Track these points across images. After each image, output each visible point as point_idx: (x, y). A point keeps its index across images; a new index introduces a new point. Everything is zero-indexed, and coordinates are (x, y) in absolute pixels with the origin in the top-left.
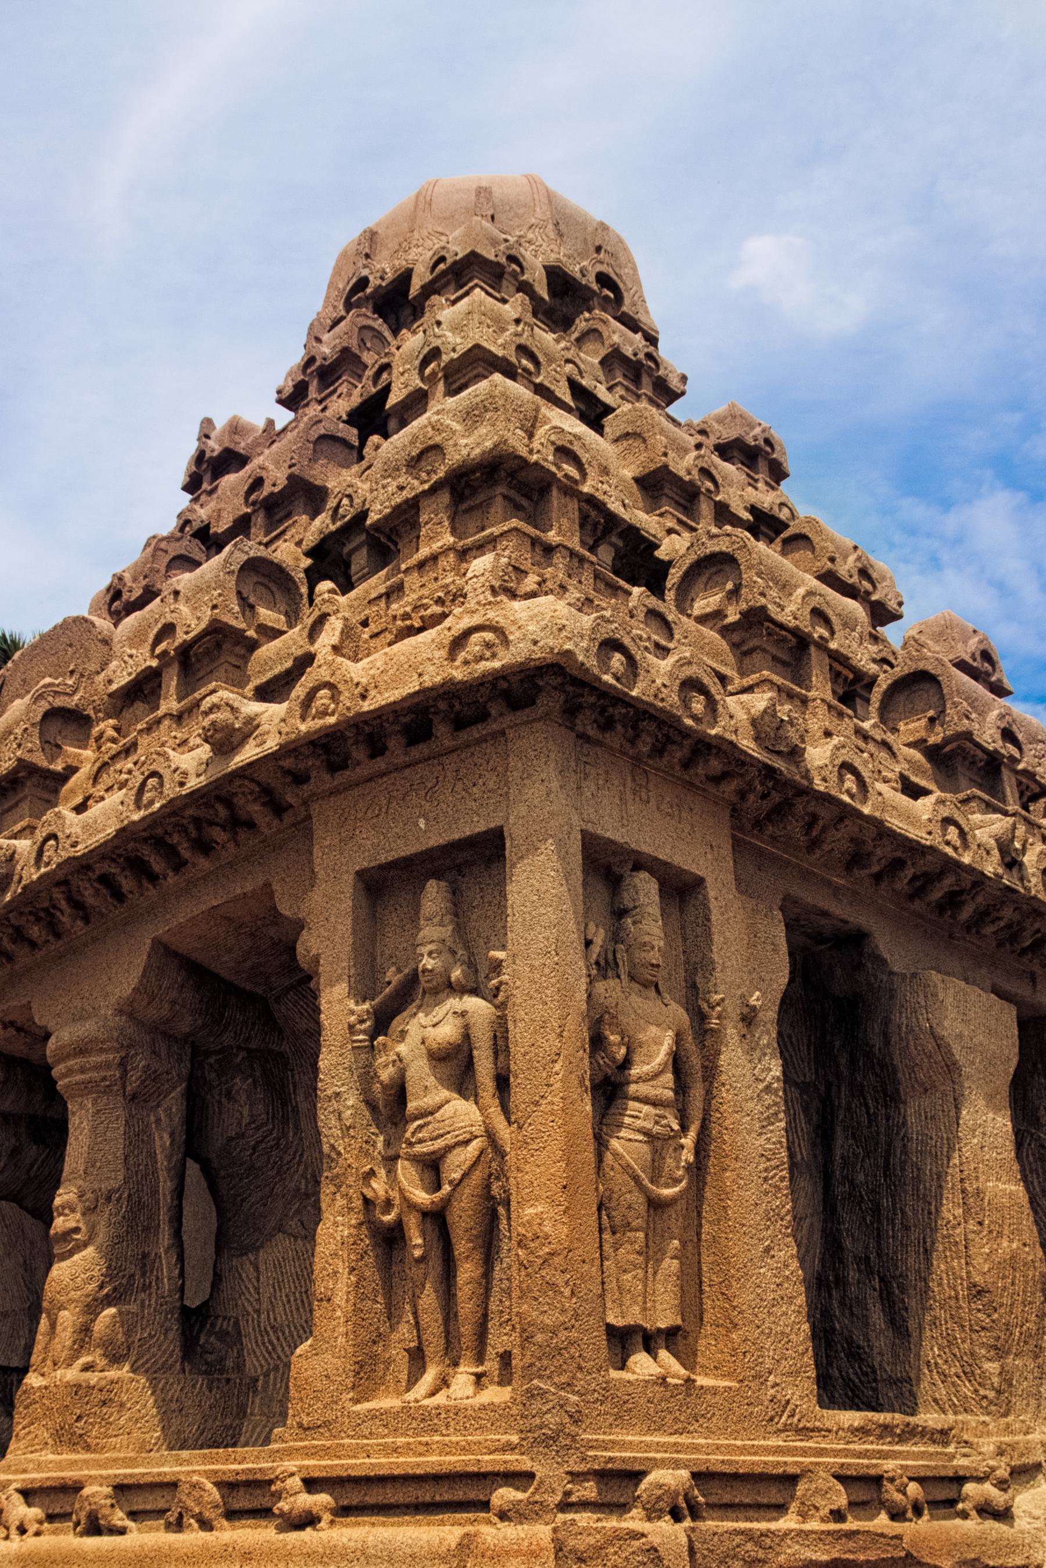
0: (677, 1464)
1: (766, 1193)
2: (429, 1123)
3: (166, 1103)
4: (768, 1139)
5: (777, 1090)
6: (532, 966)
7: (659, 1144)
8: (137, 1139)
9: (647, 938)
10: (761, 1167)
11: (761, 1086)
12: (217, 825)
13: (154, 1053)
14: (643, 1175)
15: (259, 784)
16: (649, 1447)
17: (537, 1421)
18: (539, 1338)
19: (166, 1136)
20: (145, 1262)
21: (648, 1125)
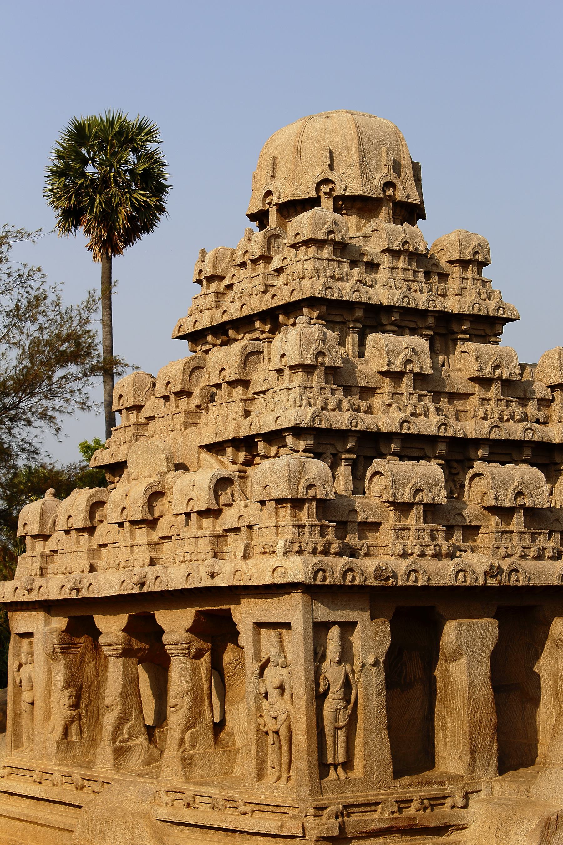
0: (338, 804)
8: (195, 672)
16: (331, 799)
17: (300, 794)
18: (300, 772)
20: (200, 713)
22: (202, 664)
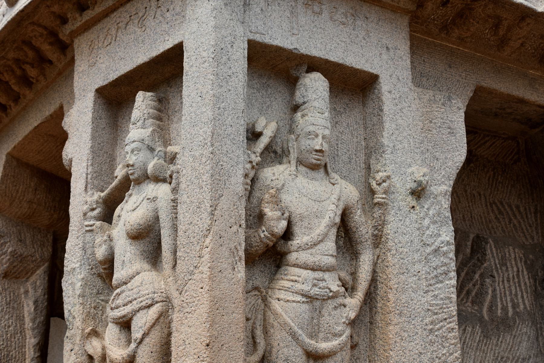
1: (432, 343)
2: (122, 292)
3: (33, 278)
4: (435, 296)
5: (445, 254)
6: (194, 156)
7: (317, 304)
9: (311, 128)
10: (427, 320)
11: (429, 250)
12: (27, 63)
13: (21, 241)
14: (300, 332)
15: (45, 28)
19: (31, 303)
21: (306, 288)
22: (26, 292)
